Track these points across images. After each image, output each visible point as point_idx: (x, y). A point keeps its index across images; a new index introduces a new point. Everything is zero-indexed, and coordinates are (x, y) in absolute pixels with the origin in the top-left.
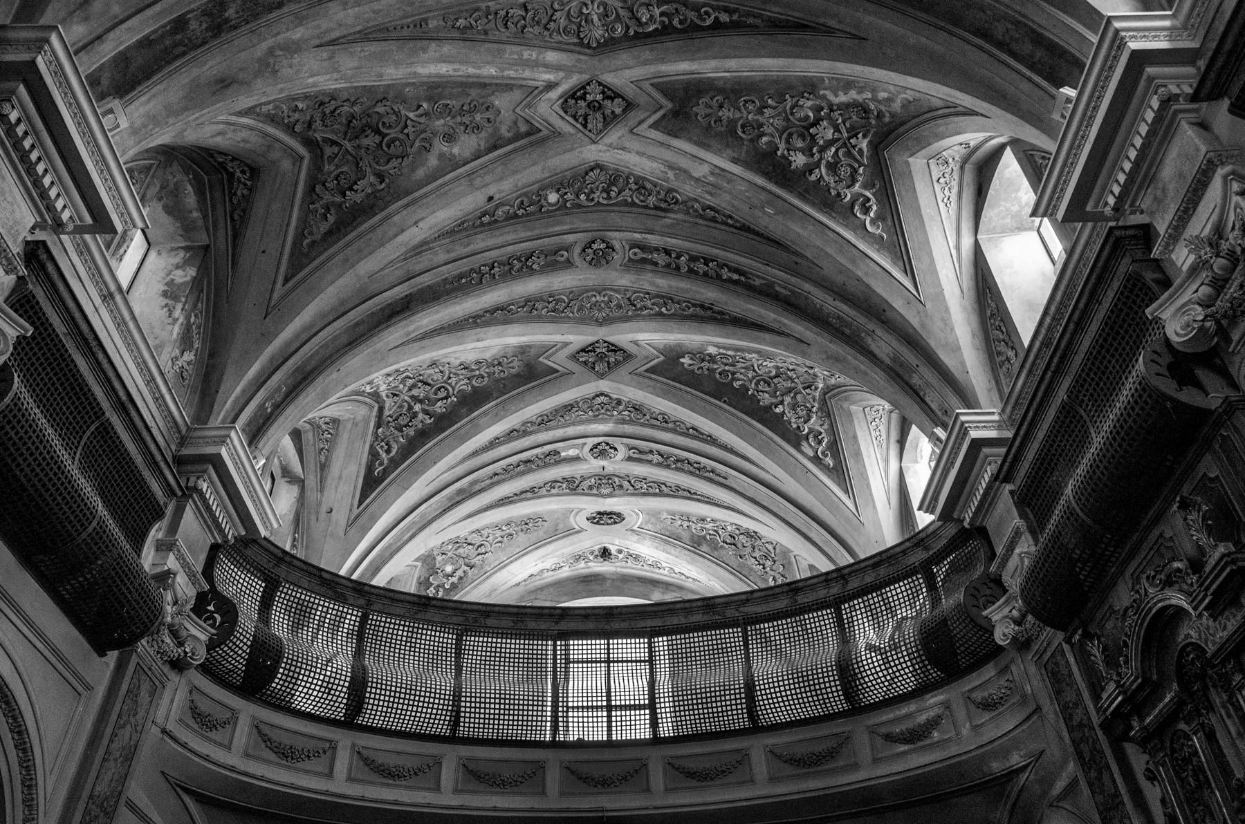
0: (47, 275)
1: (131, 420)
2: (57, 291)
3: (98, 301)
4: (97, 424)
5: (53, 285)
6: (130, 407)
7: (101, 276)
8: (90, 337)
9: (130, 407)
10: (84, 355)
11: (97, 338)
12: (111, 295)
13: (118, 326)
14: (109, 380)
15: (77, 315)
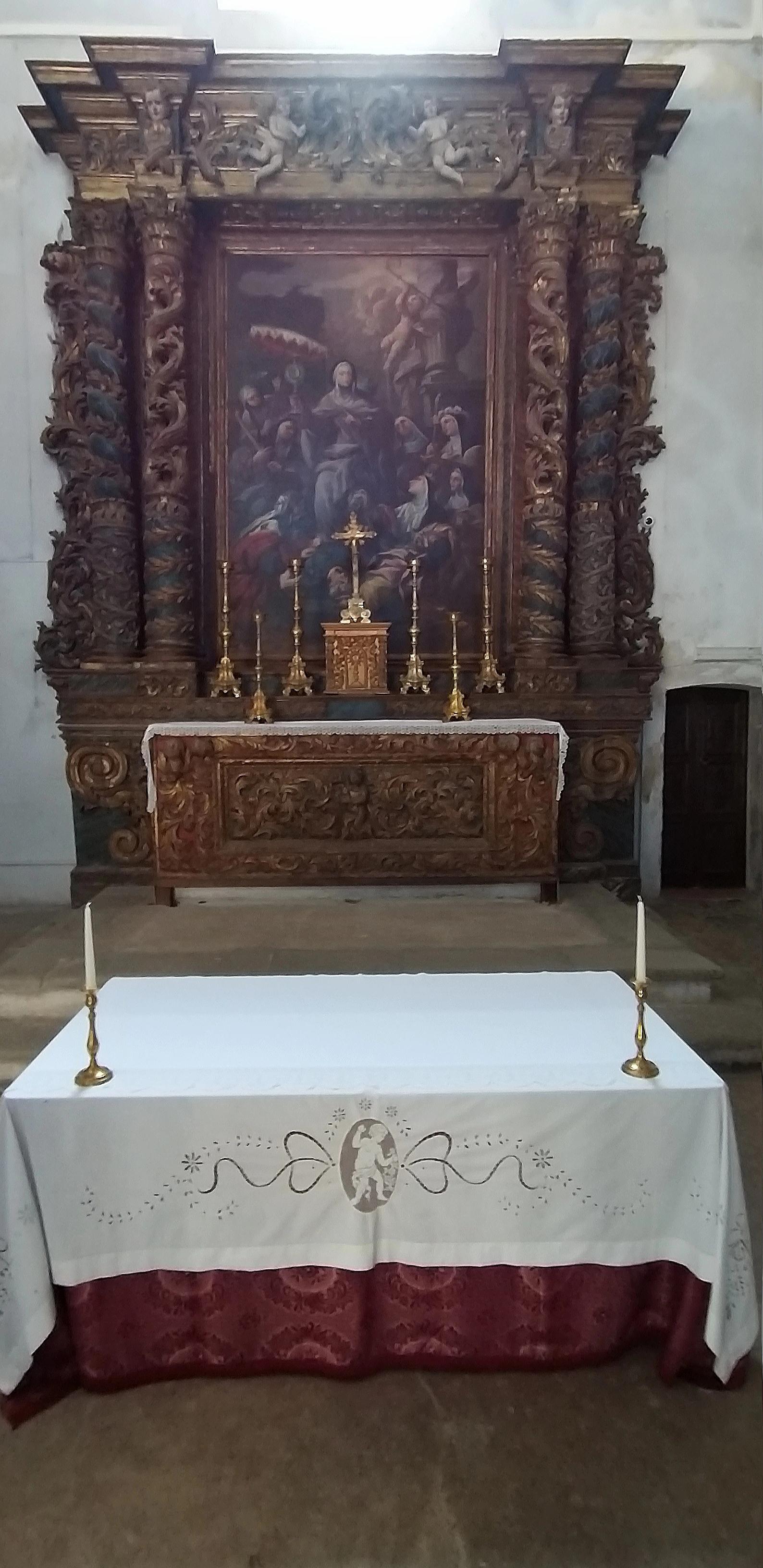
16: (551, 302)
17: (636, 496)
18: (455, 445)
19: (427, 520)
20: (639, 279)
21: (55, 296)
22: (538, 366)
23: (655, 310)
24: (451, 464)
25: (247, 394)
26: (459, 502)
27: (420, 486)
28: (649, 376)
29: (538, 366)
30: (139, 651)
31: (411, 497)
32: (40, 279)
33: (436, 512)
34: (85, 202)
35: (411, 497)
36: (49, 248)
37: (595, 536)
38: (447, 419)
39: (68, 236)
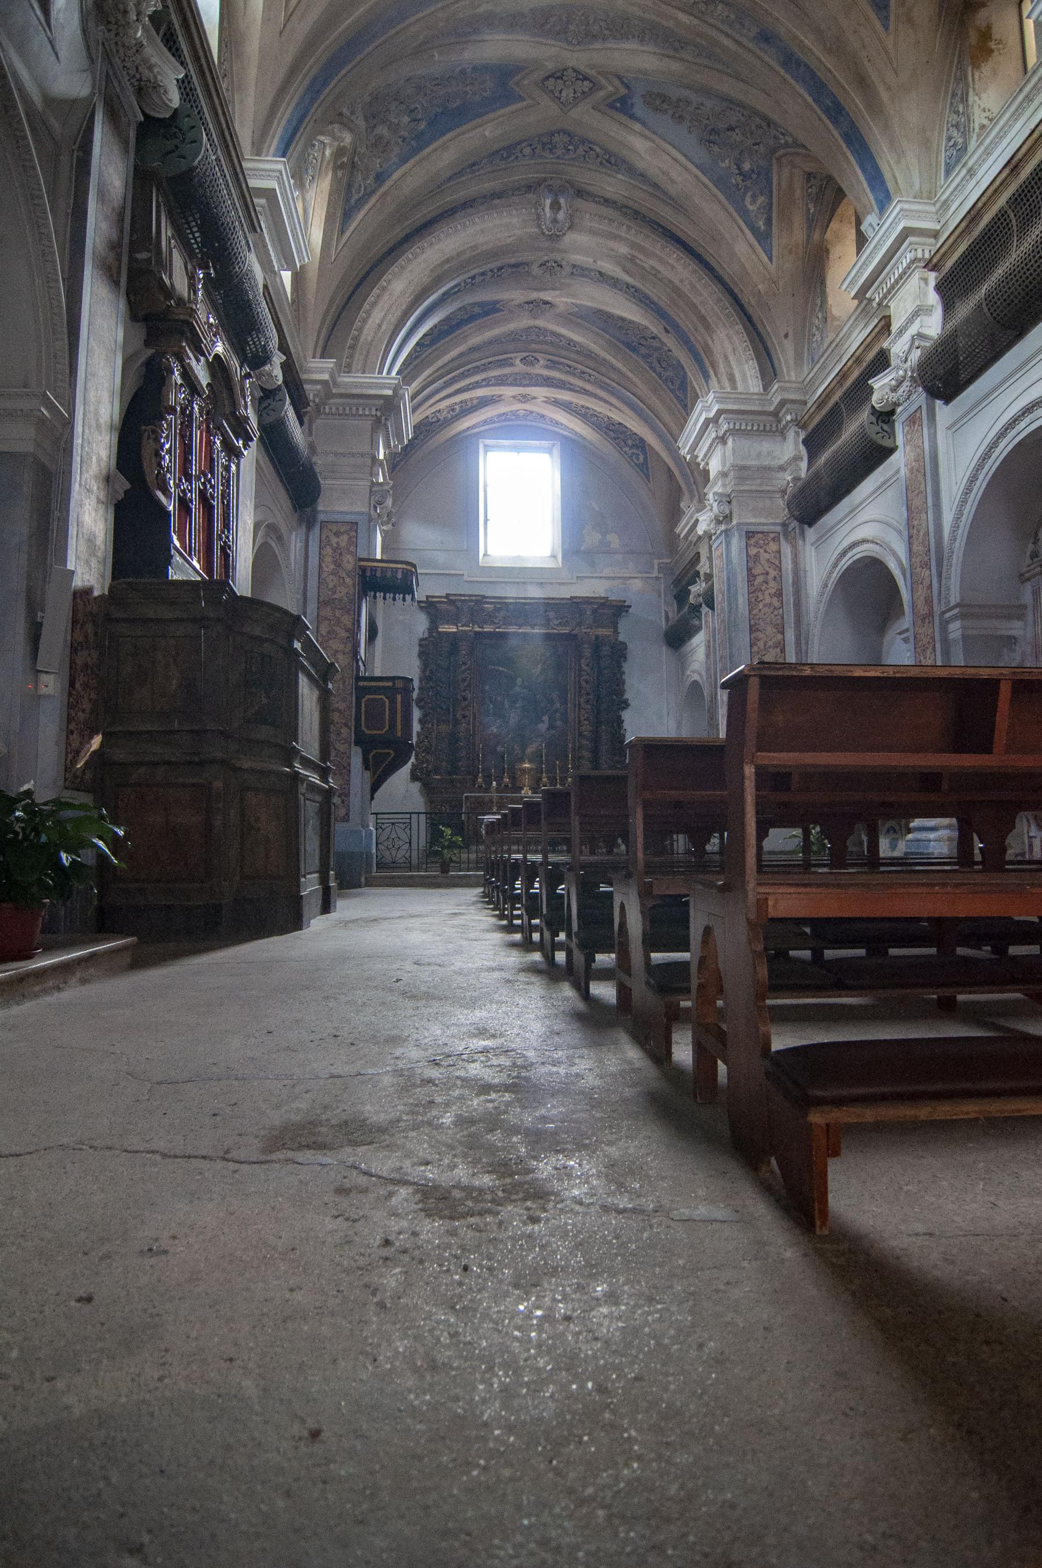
0: (939, 261)
1: (1025, 155)
2: (946, 252)
3: (973, 182)
4: (1010, 212)
5: (943, 255)
6: (1014, 162)
7: (958, 186)
8: (969, 217)
9: (1014, 162)
10: (981, 217)
11: (969, 212)
12: (969, 171)
13: (989, 154)
14: (995, 191)
15: (957, 233)
16: (587, 665)
17: (620, 722)
18: (558, 705)
19: (548, 729)
20: (620, 652)
21: (421, 654)
22: (583, 684)
23: (625, 661)
24: (556, 711)
25: (487, 687)
26: (559, 723)
27: (546, 718)
28: (624, 682)
29: (583, 684)
30: (450, 774)
31: (542, 722)
32: (416, 650)
33: (551, 727)
34: (439, 632)
35: (542, 722)
36: (421, 640)
37: (605, 737)
38: (555, 695)
39: (426, 635)
